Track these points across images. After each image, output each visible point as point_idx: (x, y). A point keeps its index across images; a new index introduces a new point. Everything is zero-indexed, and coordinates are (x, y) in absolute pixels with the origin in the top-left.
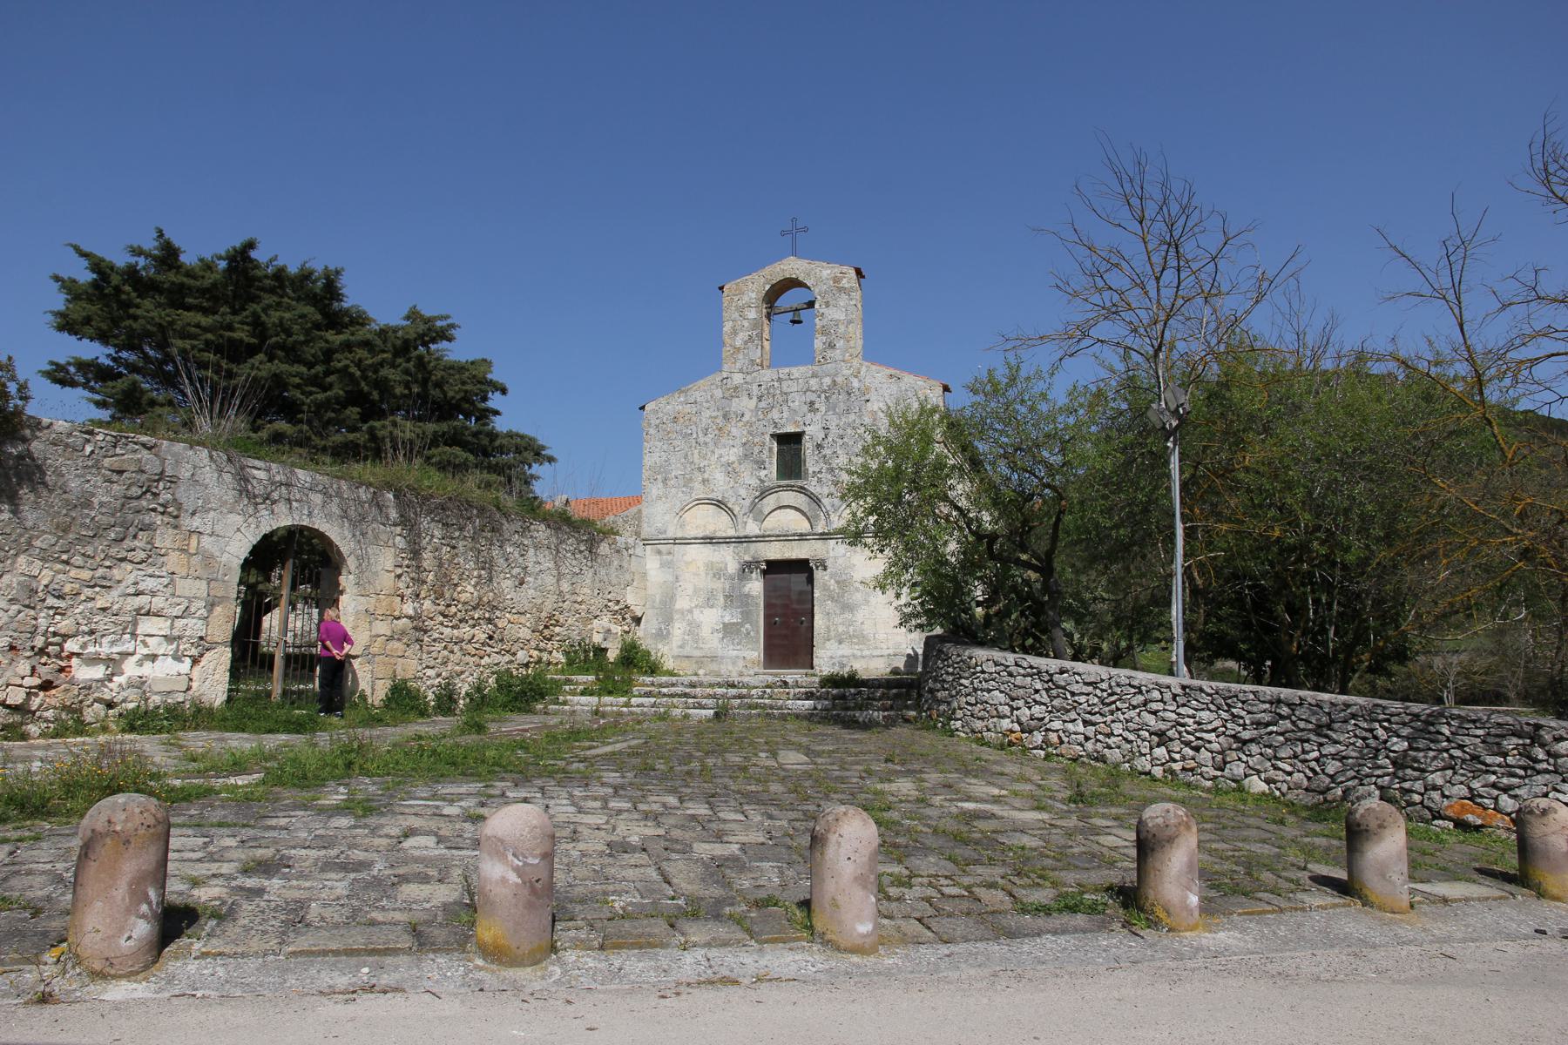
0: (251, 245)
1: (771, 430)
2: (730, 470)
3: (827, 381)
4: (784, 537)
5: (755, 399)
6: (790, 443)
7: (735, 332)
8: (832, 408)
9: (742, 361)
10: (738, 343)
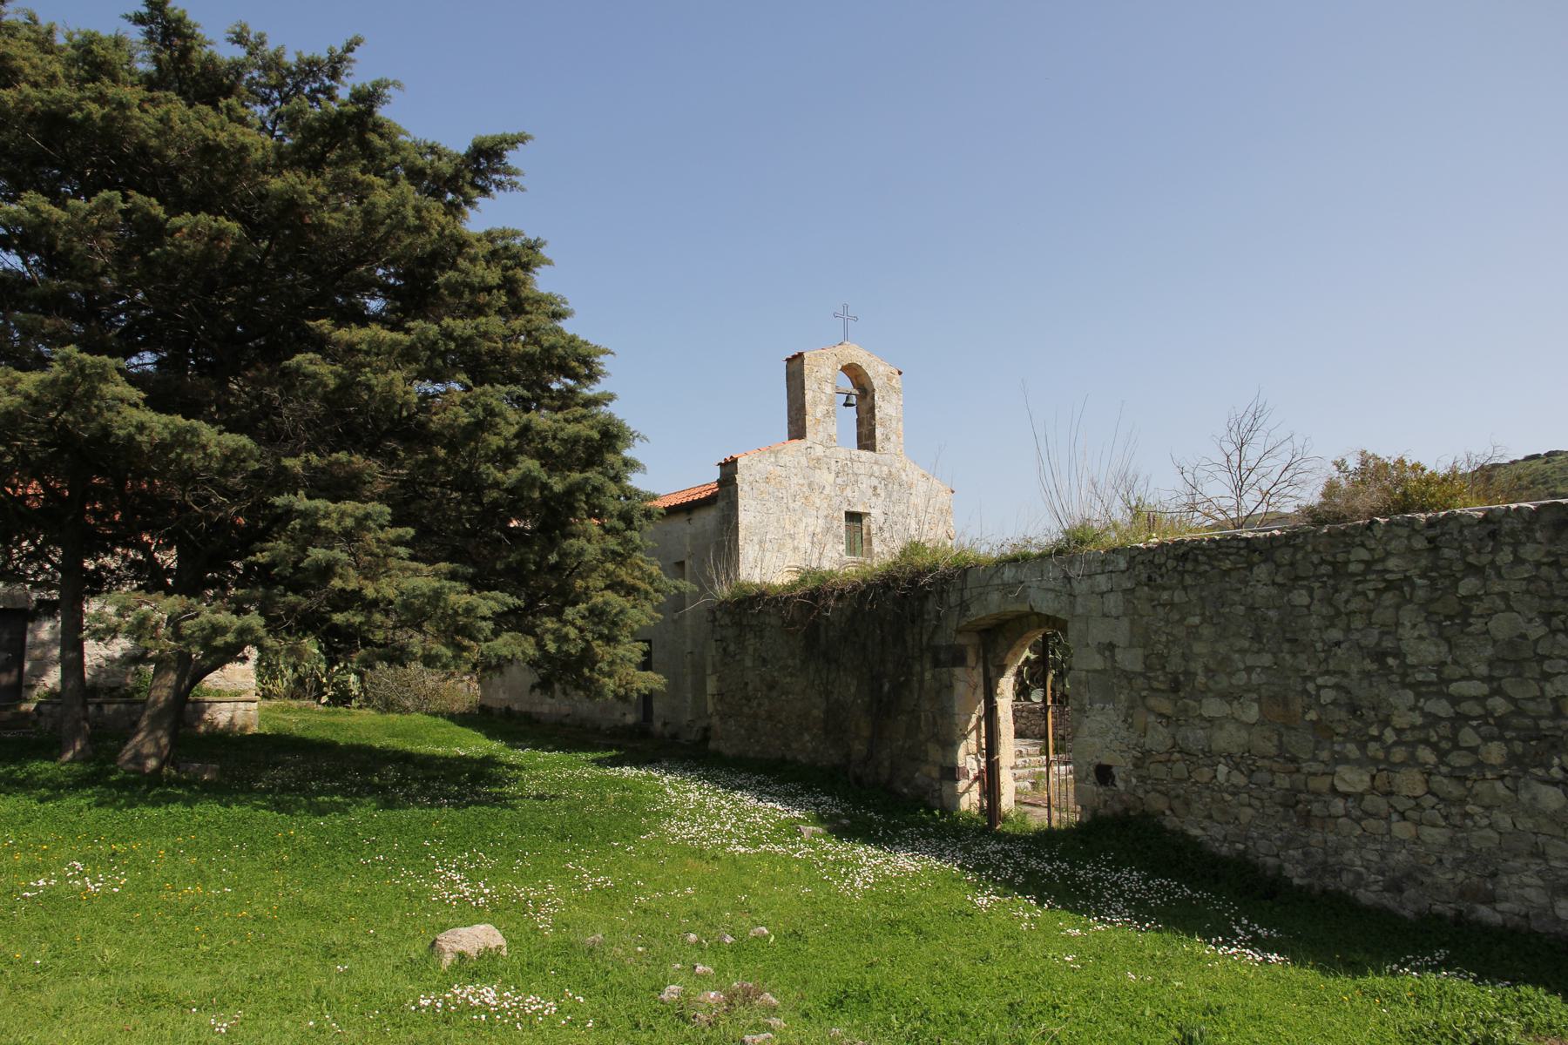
0: (516, 141)
1: (846, 508)
3: (885, 469)
5: (833, 475)
6: (854, 517)
7: (815, 404)
9: (822, 436)
10: (819, 415)
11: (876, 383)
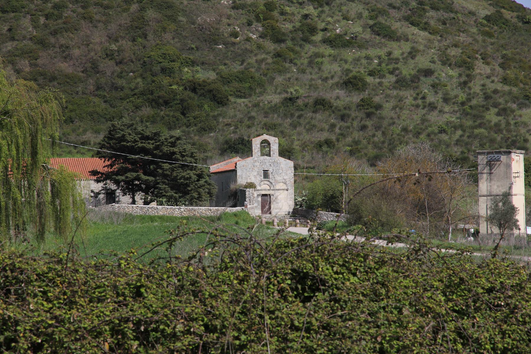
2: (255, 177)
4: (265, 190)
8: (274, 166)
11: (271, 143)
